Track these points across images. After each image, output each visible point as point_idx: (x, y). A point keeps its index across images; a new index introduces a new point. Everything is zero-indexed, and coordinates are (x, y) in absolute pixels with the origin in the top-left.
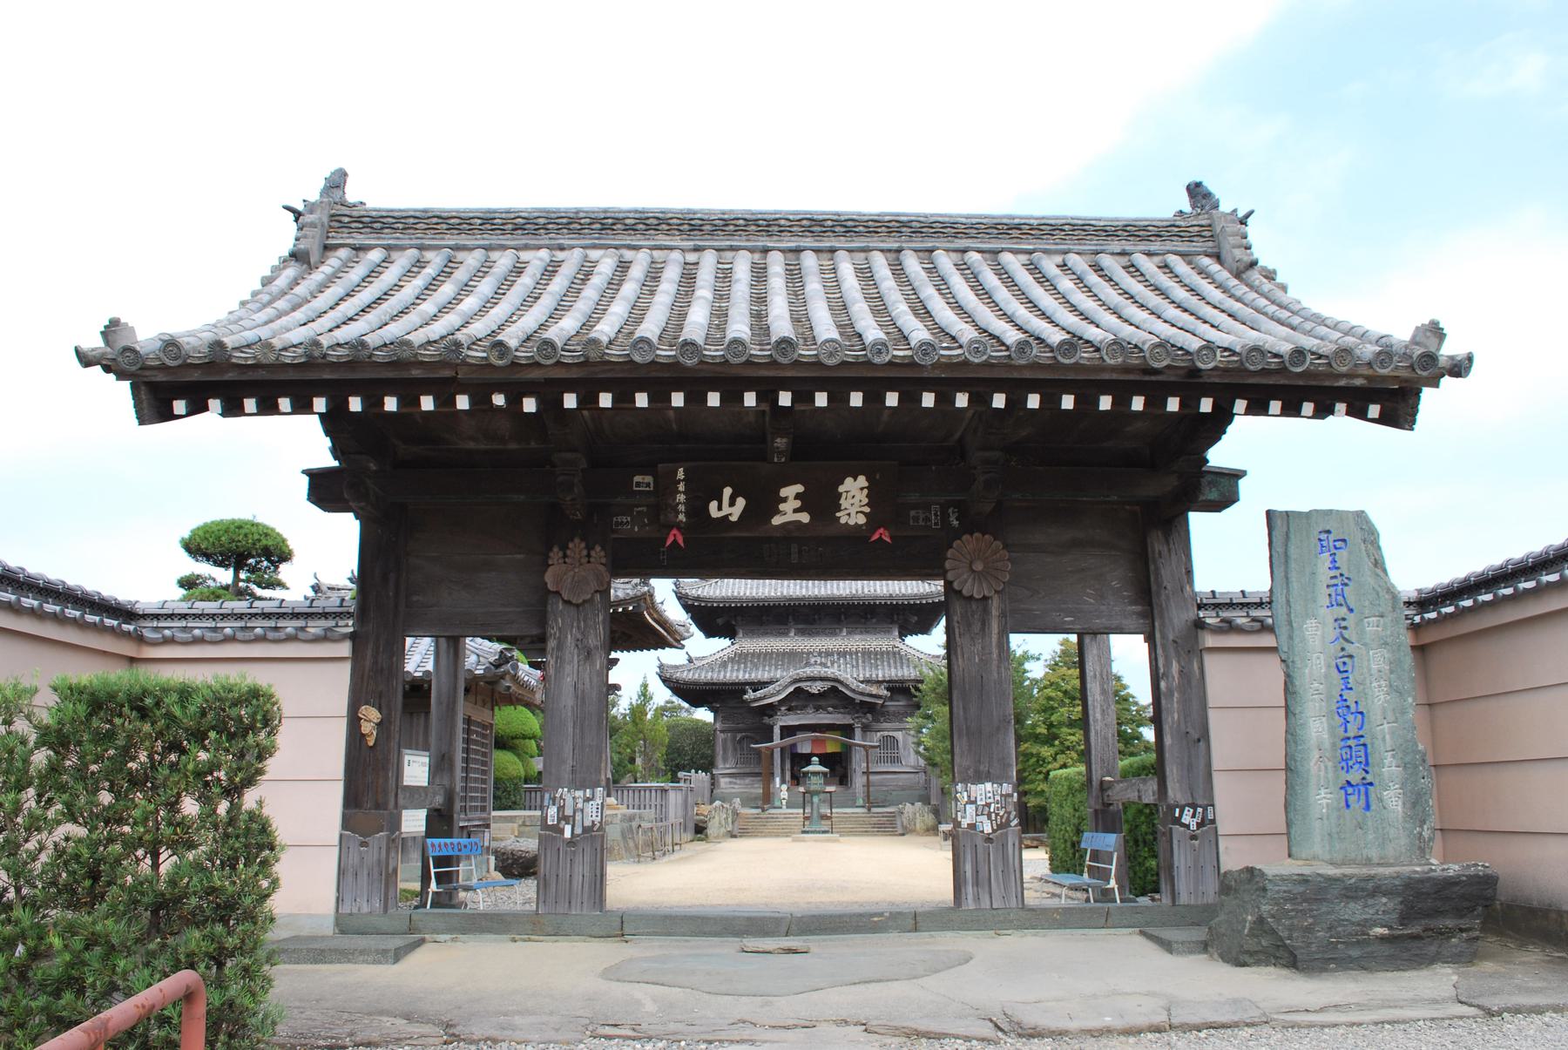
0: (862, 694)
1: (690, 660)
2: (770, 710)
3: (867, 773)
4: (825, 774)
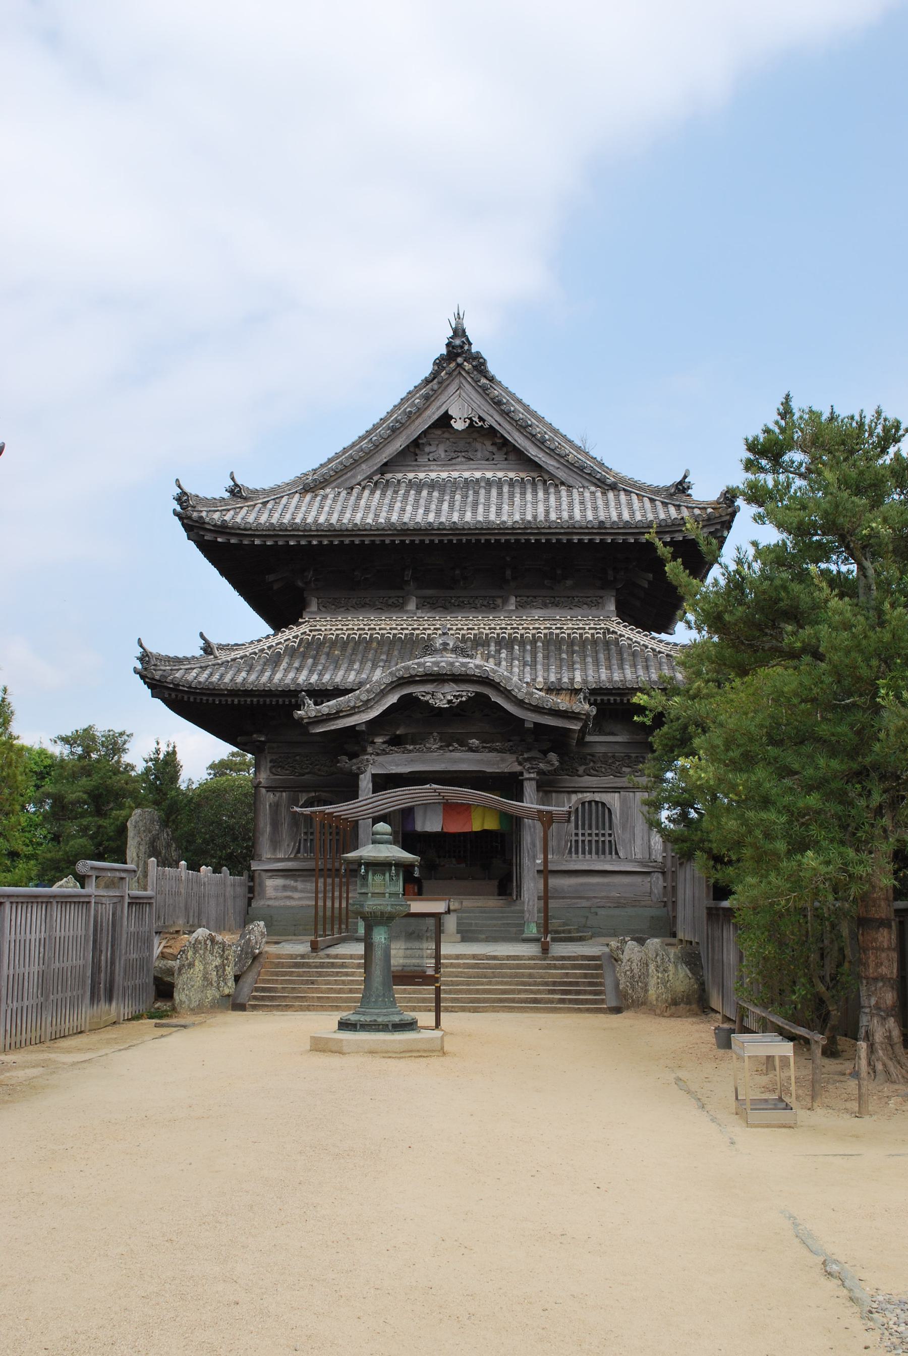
0: (537, 709)
1: (208, 649)
2: (352, 741)
3: (545, 873)
4: (406, 868)
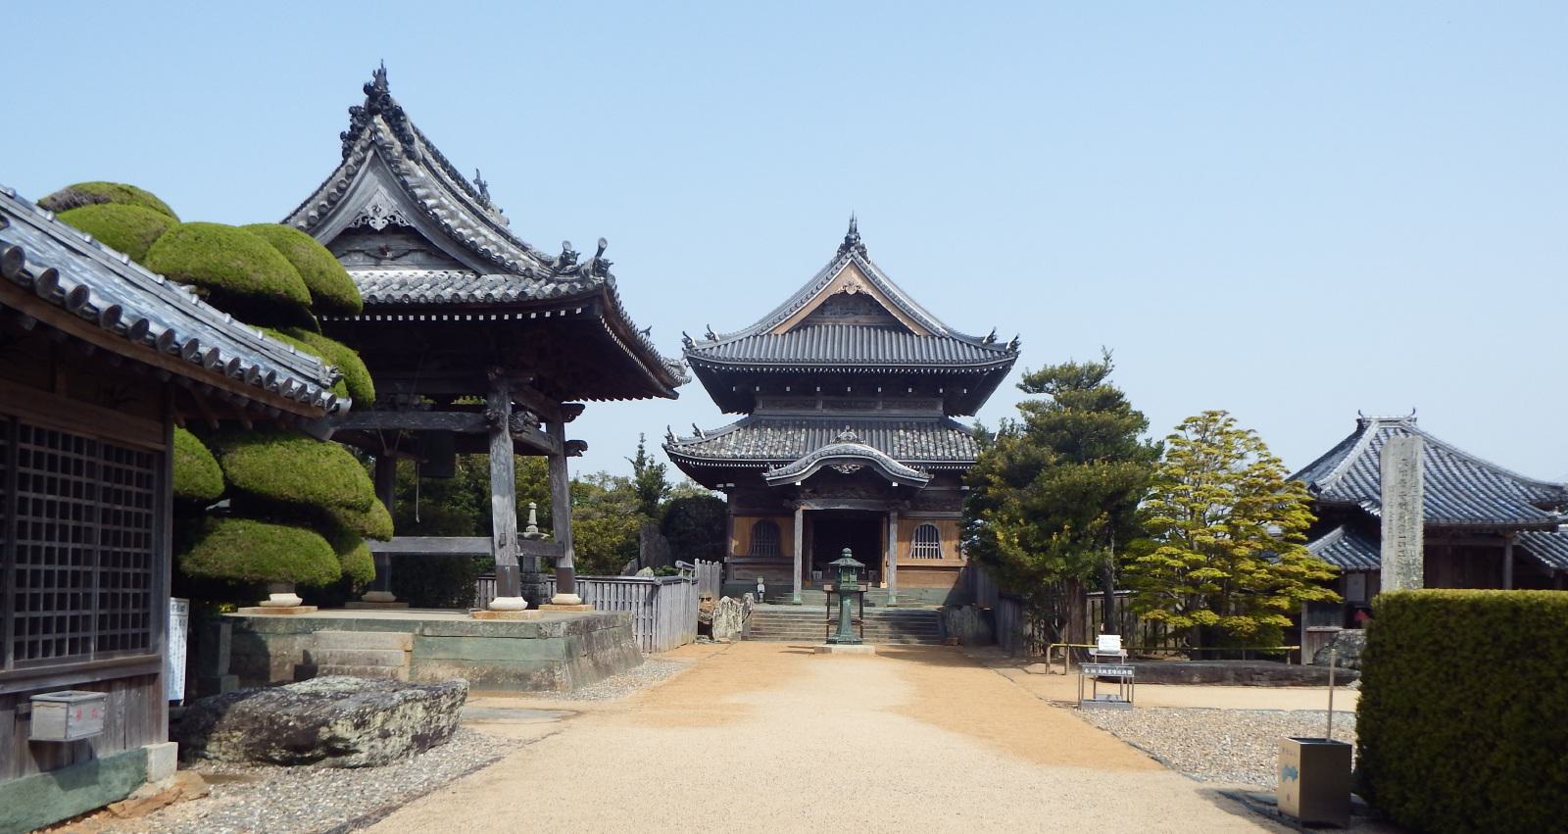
4: (859, 569)
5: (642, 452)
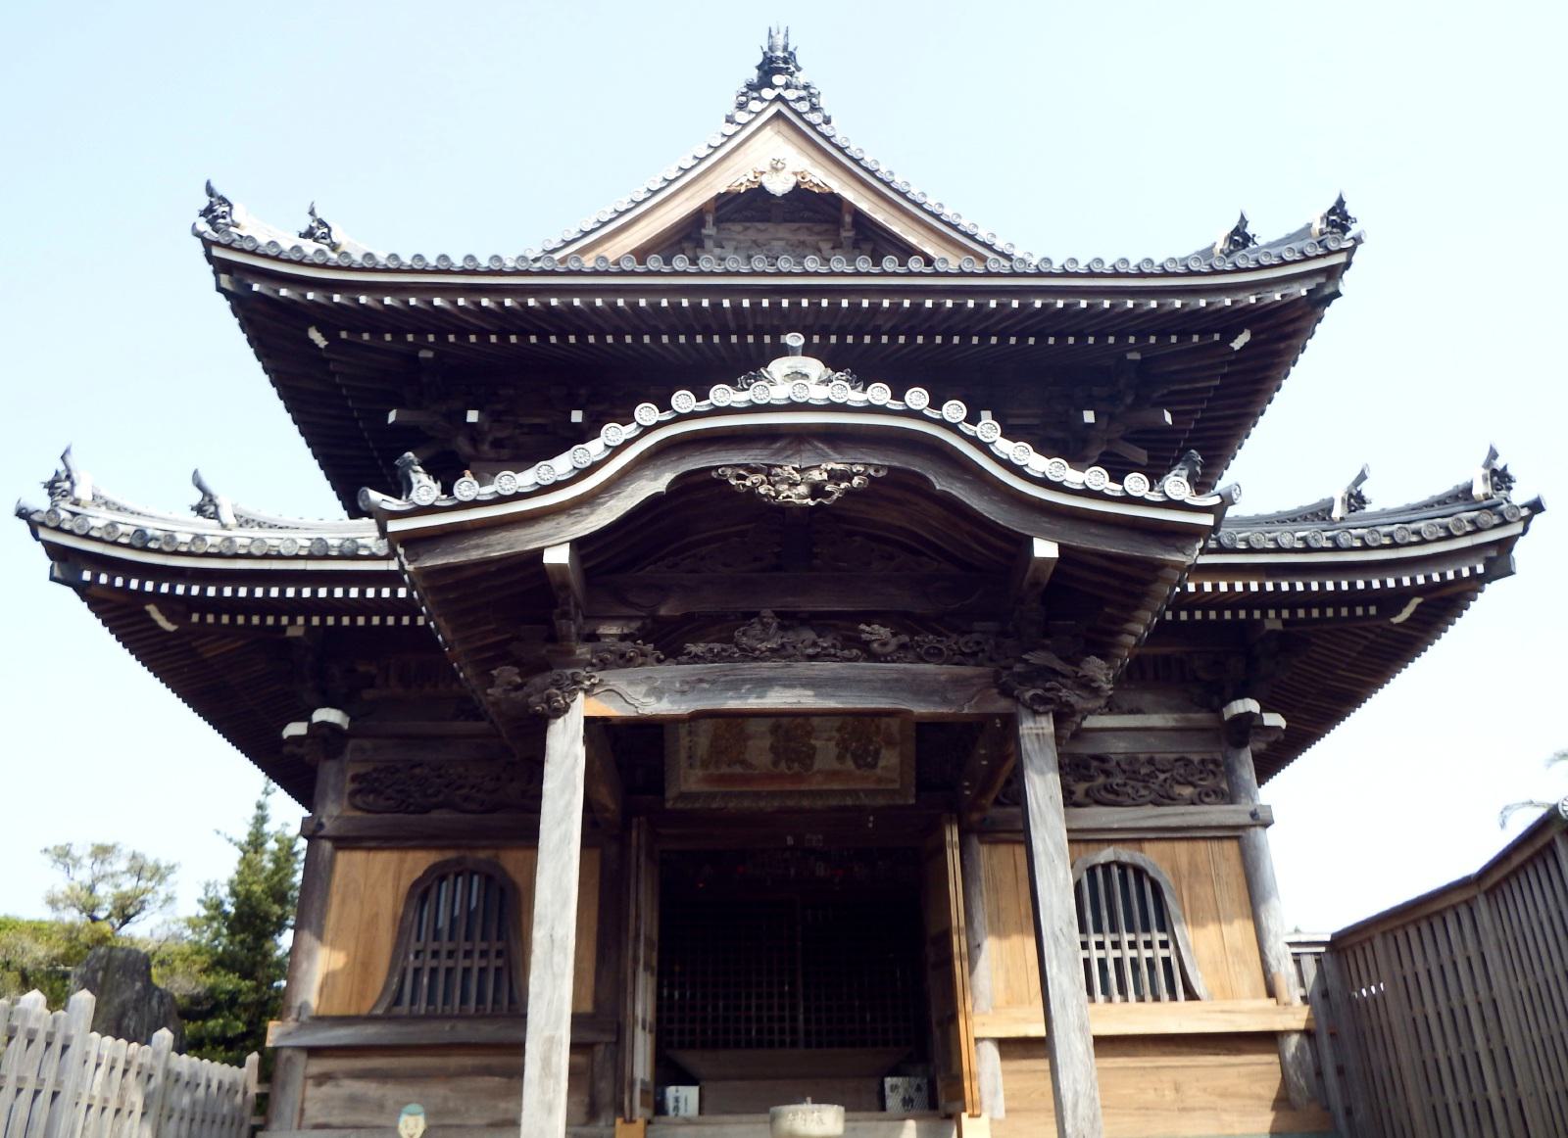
5: (261, 820)
